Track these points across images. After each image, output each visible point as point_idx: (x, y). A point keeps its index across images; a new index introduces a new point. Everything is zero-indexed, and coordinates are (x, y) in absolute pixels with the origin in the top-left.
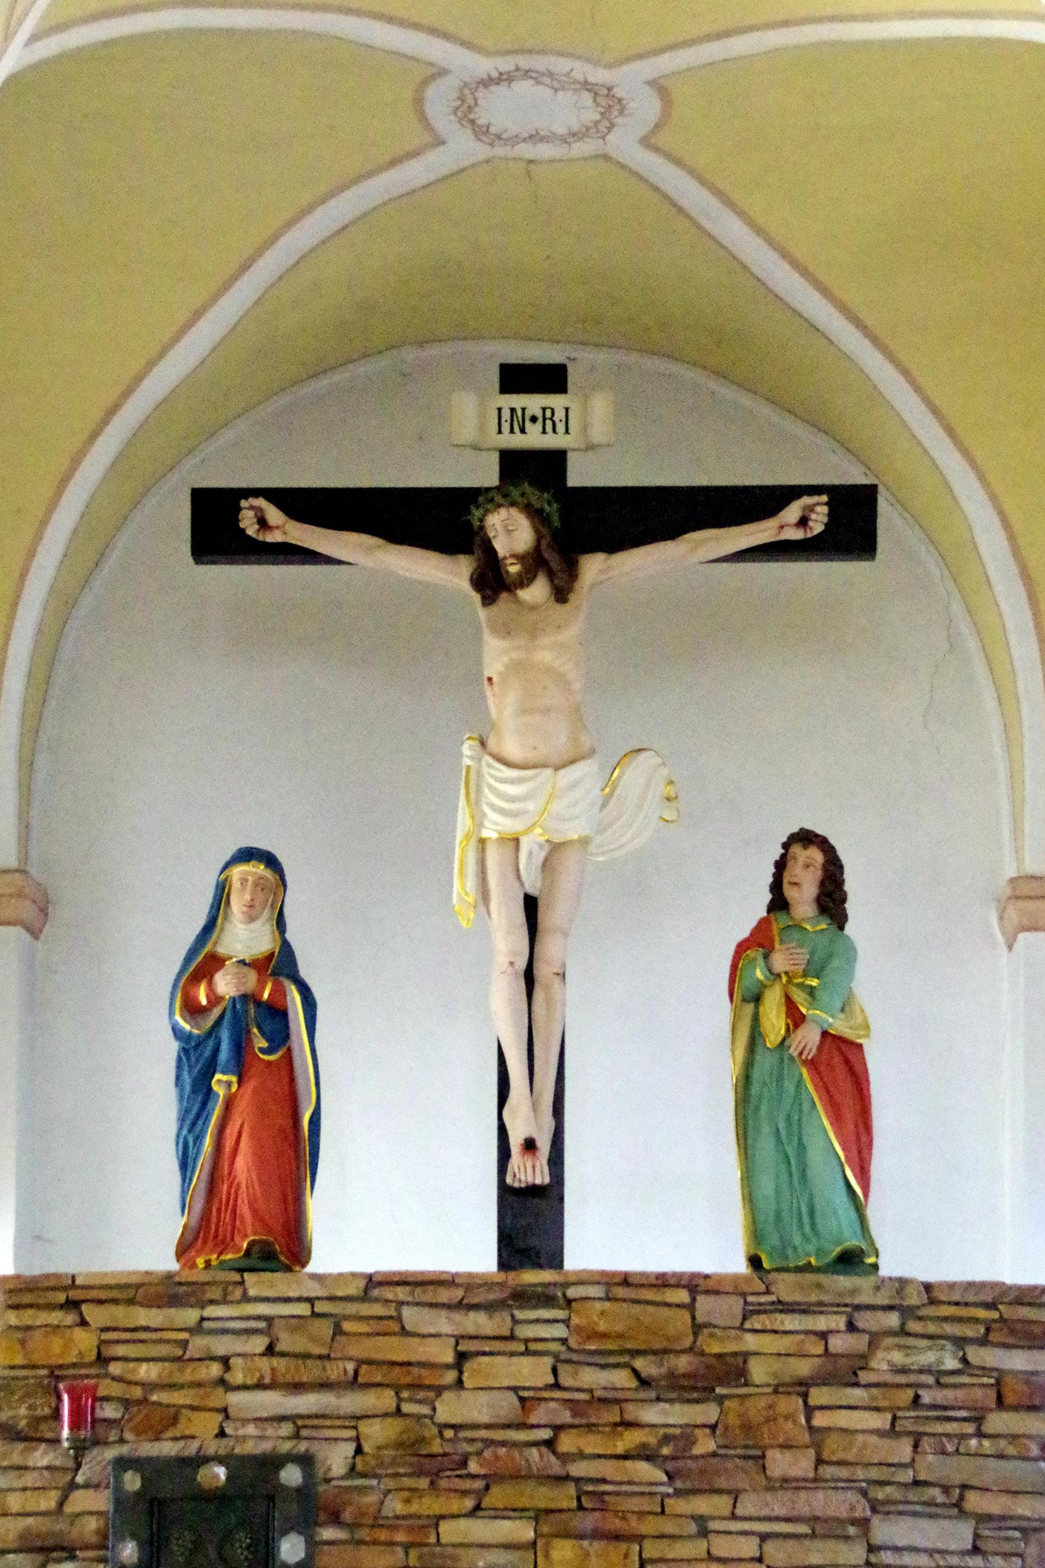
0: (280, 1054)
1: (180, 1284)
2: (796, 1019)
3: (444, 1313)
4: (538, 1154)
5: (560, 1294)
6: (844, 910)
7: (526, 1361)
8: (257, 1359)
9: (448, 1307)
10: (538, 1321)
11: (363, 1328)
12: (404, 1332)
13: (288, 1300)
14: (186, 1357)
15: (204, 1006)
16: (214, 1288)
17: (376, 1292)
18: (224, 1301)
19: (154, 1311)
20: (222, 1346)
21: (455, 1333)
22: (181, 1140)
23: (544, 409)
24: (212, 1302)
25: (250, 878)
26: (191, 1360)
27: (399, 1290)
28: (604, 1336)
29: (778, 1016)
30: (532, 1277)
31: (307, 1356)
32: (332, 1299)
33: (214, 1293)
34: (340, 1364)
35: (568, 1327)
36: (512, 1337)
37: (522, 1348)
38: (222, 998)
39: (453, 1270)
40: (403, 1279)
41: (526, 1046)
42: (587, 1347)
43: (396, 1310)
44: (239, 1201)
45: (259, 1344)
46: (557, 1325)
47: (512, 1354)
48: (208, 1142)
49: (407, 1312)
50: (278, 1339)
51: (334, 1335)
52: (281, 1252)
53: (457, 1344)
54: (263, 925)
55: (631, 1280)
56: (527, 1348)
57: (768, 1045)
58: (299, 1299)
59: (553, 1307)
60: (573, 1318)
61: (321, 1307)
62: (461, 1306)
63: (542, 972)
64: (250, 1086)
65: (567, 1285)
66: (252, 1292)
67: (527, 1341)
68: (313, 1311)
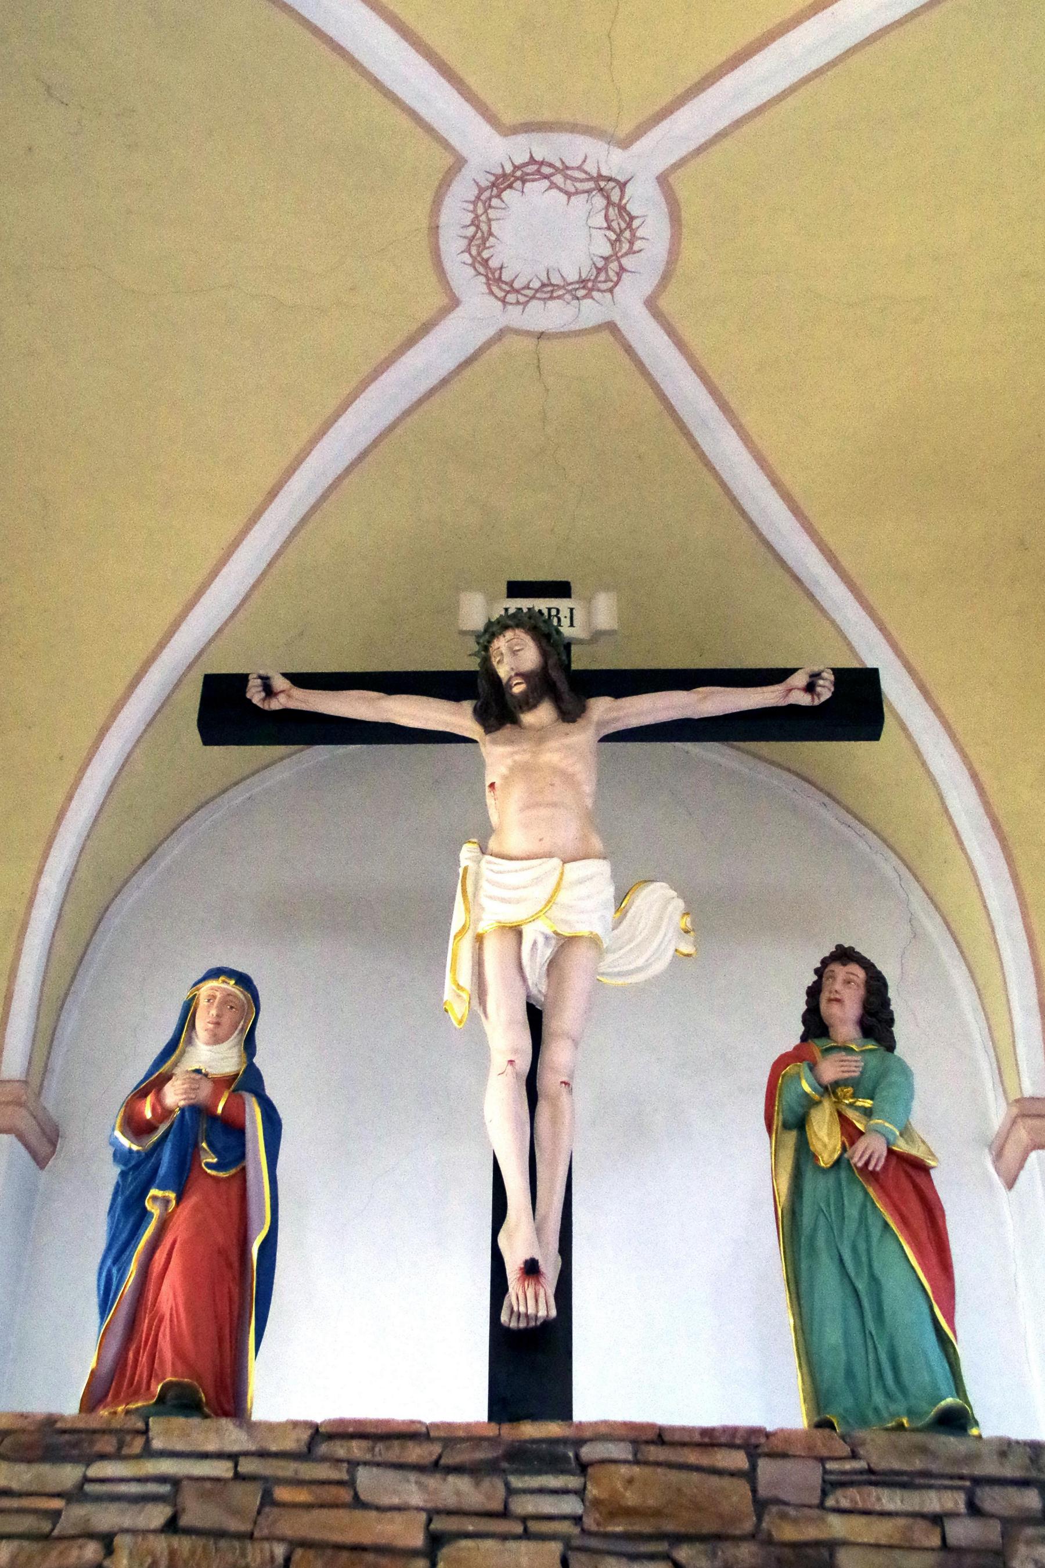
0: (233, 1171)
1: (64, 1432)
2: (851, 1134)
3: (413, 1476)
4: (542, 1280)
5: (571, 1454)
6: (892, 1033)
7: (524, 1546)
8: (151, 1537)
9: (419, 1468)
10: (541, 1491)
11: (302, 1496)
12: (358, 1503)
13: (205, 1456)
14: (56, 1532)
15: (148, 1121)
16: (106, 1437)
17: (323, 1448)
18: (117, 1456)
19: (22, 1467)
20: (106, 1518)
21: (429, 1505)
22: (104, 1274)
23: (549, 609)
24: (103, 1457)
25: (218, 995)
26: (61, 1538)
27: (354, 1444)
28: (629, 1512)
29: (829, 1135)
30: (530, 1430)
31: (220, 1534)
32: (263, 1454)
33: (106, 1444)
34: (266, 1545)
35: (583, 1501)
36: (504, 1514)
37: (519, 1529)
38: (171, 1112)
39: (428, 1419)
40: (361, 1429)
41: (527, 1160)
42: (610, 1529)
43: (348, 1471)
44: (160, 1335)
45: (157, 1515)
46: (566, 1497)
47: (505, 1537)
48: (133, 1269)
49: (363, 1476)
50: (184, 1510)
51: (262, 1505)
52: (208, 1403)
53: (430, 1521)
54: (230, 1048)
55: (667, 1438)
56: (526, 1529)
57: (822, 1164)
58: (220, 1456)
59: (563, 1472)
60: (589, 1487)
61: (247, 1466)
62: (436, 1467)
63: (548, 1082)
64: (193, 1200)
65: (579, 1442)
66: (157, 1444)
67: (524, 1519)
68: (236, 1473)
